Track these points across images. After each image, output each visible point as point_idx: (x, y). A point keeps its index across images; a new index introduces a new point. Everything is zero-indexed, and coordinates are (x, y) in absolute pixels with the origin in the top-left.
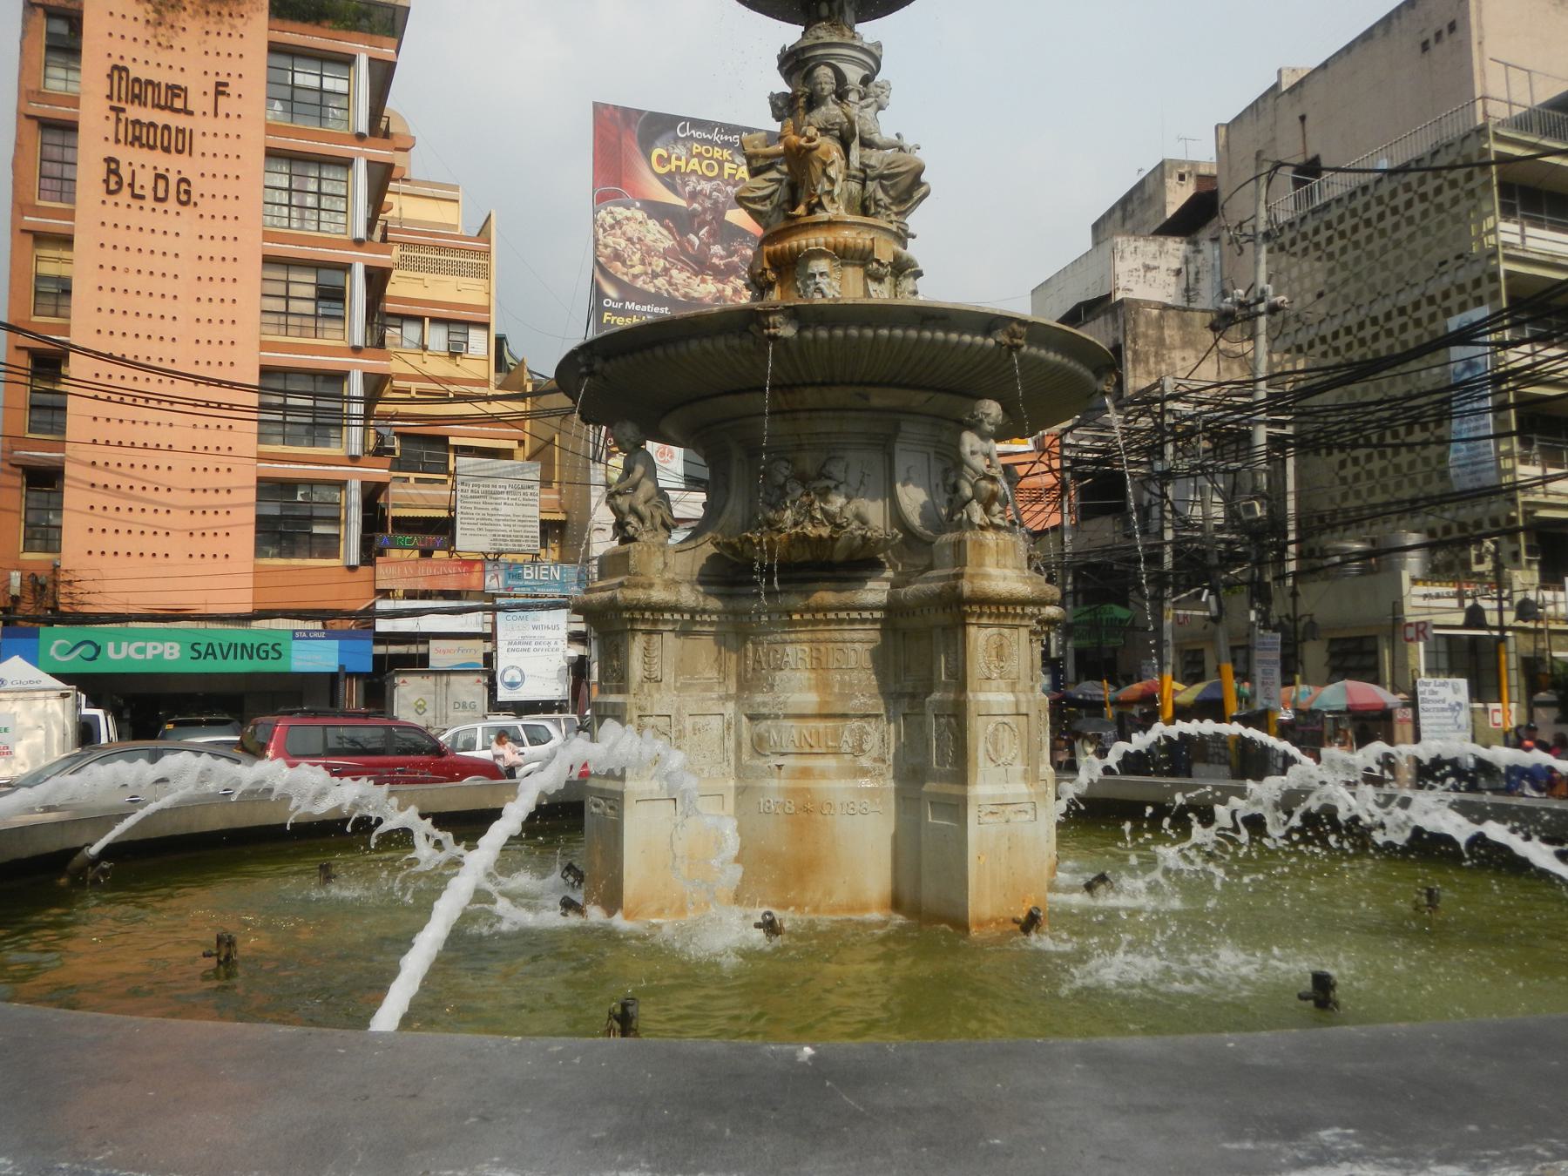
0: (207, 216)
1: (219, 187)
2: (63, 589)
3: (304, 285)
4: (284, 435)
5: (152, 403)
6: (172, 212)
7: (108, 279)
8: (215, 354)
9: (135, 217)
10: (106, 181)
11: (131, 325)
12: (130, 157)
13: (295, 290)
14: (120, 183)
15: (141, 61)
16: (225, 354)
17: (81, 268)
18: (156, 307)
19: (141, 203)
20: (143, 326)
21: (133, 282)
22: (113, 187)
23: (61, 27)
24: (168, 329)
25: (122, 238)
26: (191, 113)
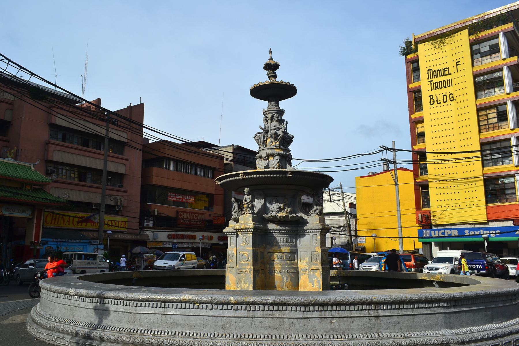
0: (459, 102)
1: (461, 92)
2: (432, 218)
3: (493, 114)
4: (492, 162)
5: (450, 162)
6: (449, 105)
7: (434, 129)
8: (466, 142)
9: (439, 109)
10: (430, 102)
11: (441, 140)
12: (434, 93)
13: (490, 116)
14: (434, 102)
15: (435, 65)
16: (469, 142)
17: (426, 128)
18: (448, 133)
19: (440, 105)
20: (445, 139)
21: (441, 128)
22: (432, 103)
23: (415, 65)
24: (452, 138)
25: (436, 116)
26: (449, 74)
